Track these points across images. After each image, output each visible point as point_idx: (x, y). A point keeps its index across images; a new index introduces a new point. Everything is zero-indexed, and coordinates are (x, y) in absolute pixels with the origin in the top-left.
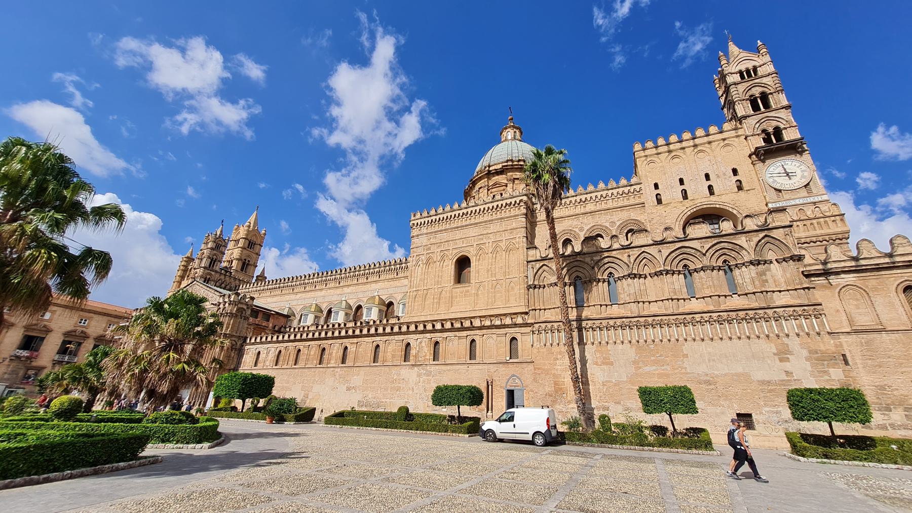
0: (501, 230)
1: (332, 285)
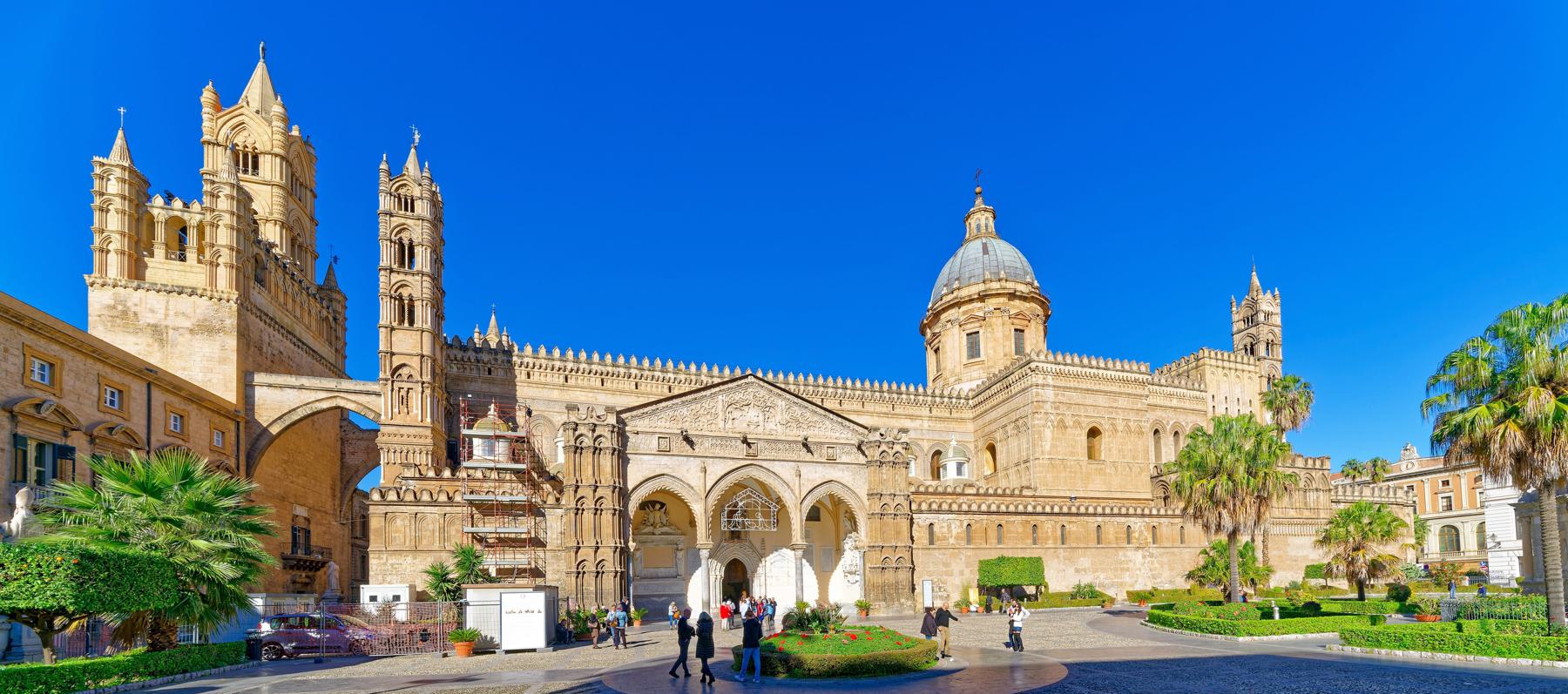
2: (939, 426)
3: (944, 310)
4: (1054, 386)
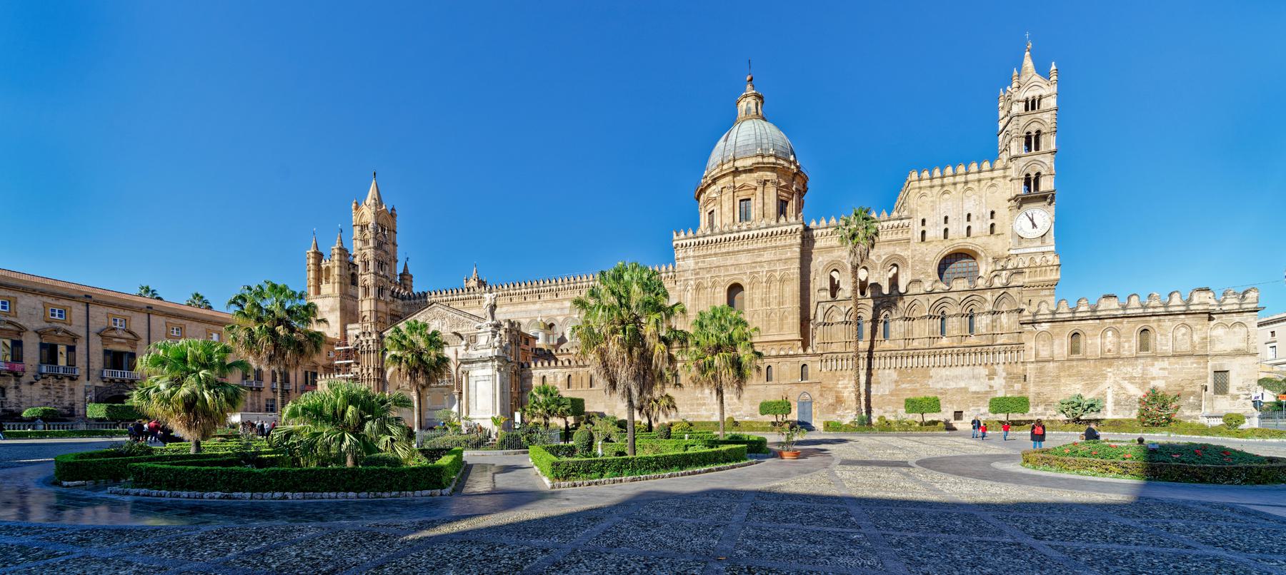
1: (547, 297)
4: (694, 257)
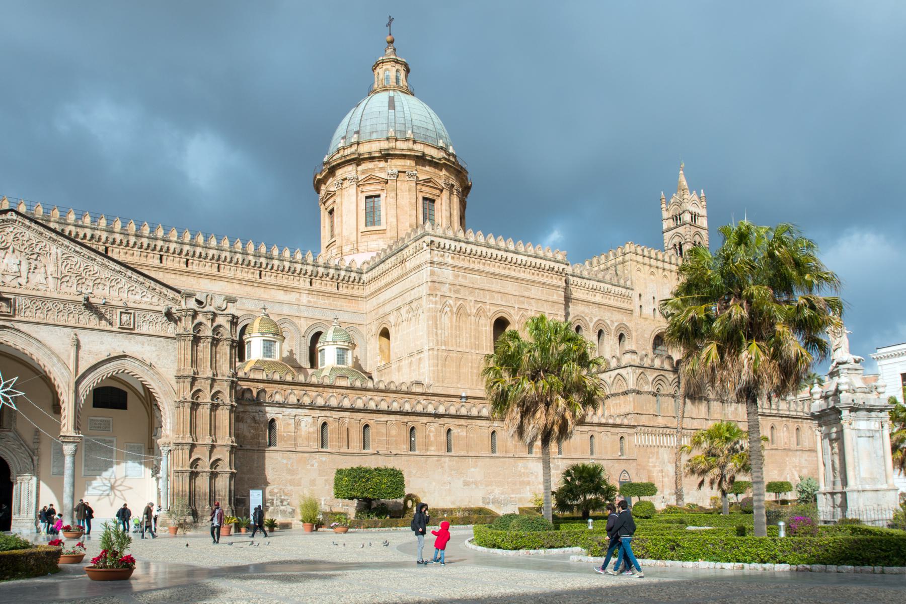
0: (543, 298)
2: (322, 302)
3: (340, 166)
